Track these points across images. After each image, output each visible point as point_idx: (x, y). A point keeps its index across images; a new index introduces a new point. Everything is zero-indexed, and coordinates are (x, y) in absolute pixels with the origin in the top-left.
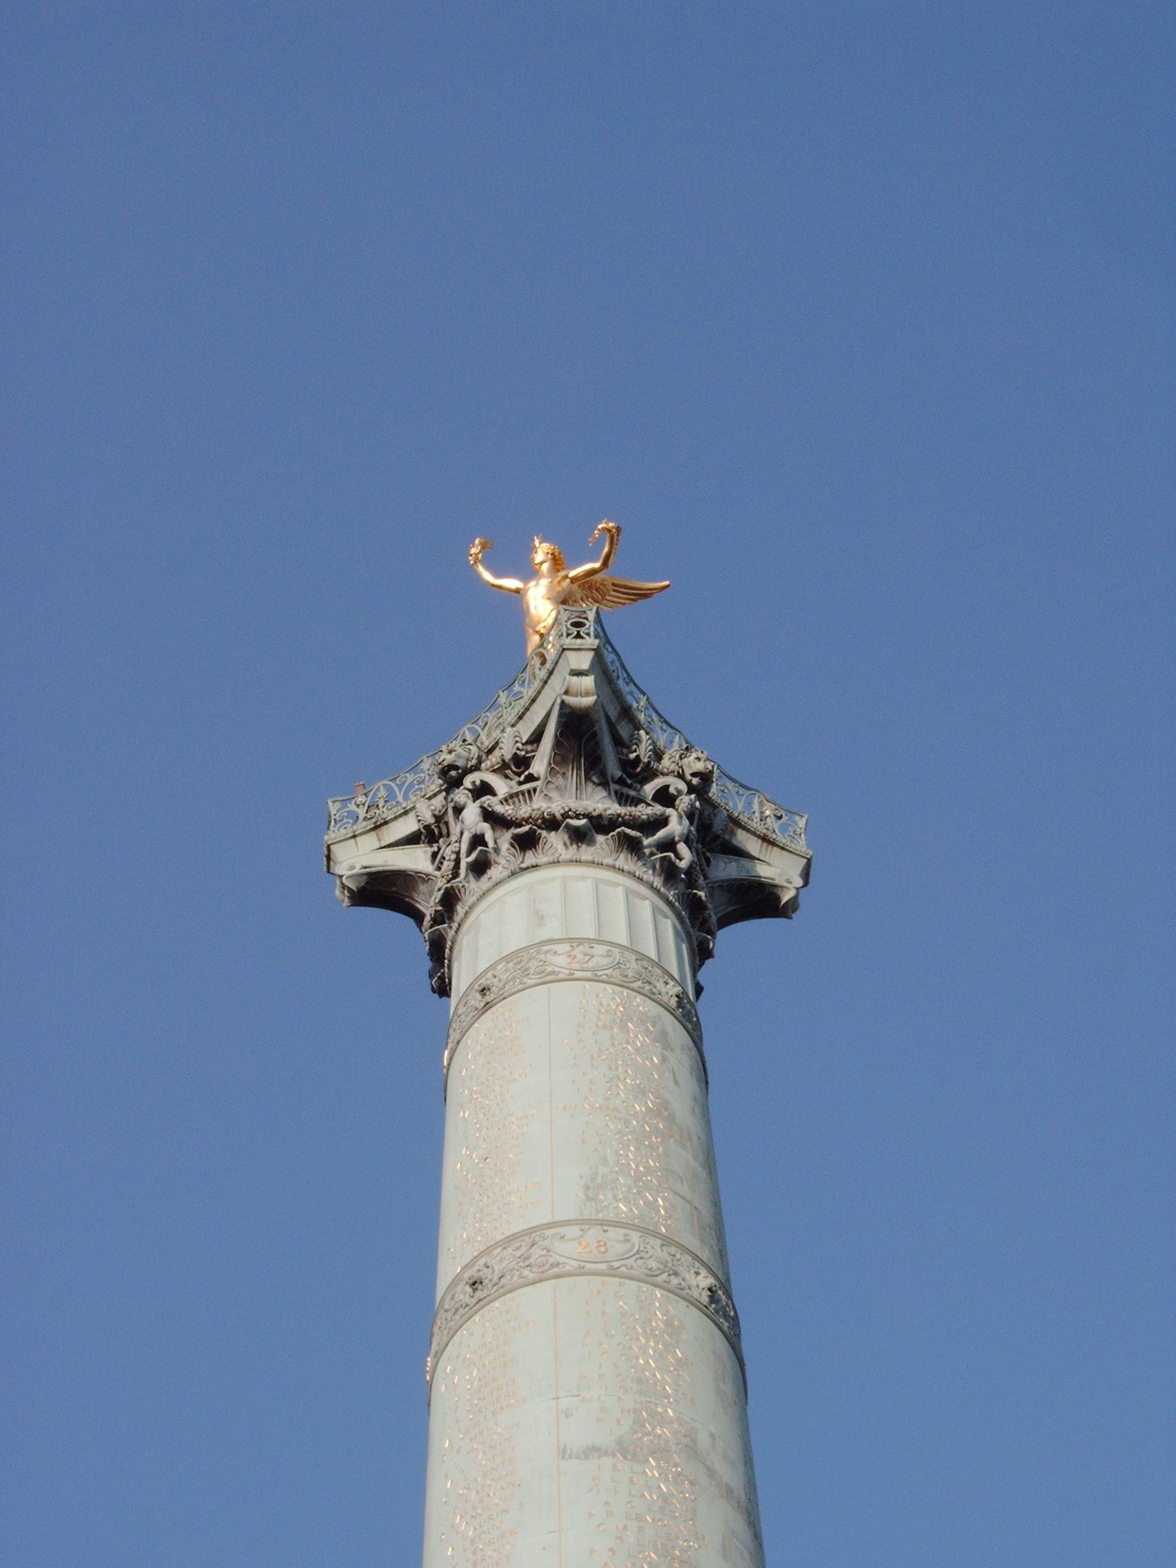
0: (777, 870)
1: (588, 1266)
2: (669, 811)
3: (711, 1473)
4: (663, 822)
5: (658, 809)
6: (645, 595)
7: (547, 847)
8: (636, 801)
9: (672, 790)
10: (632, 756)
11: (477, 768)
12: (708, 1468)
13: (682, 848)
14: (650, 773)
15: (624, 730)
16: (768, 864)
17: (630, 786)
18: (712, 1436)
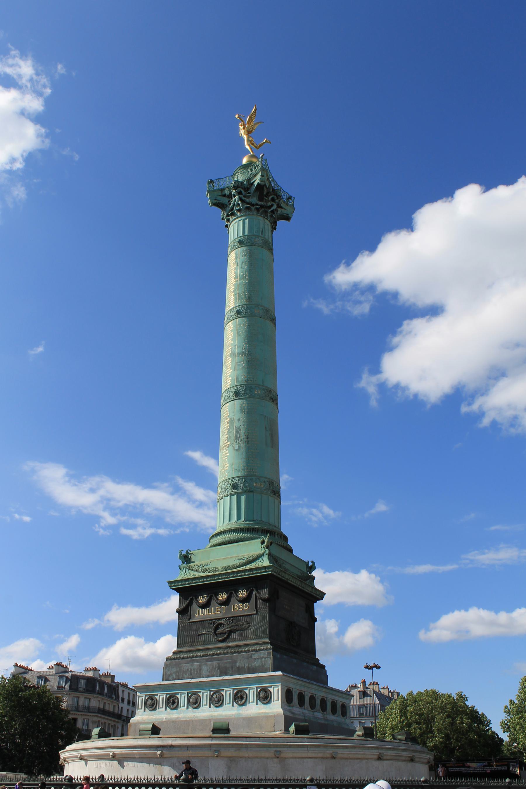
4: (272, 205)
5: (272, 203)
11: (239, 187)
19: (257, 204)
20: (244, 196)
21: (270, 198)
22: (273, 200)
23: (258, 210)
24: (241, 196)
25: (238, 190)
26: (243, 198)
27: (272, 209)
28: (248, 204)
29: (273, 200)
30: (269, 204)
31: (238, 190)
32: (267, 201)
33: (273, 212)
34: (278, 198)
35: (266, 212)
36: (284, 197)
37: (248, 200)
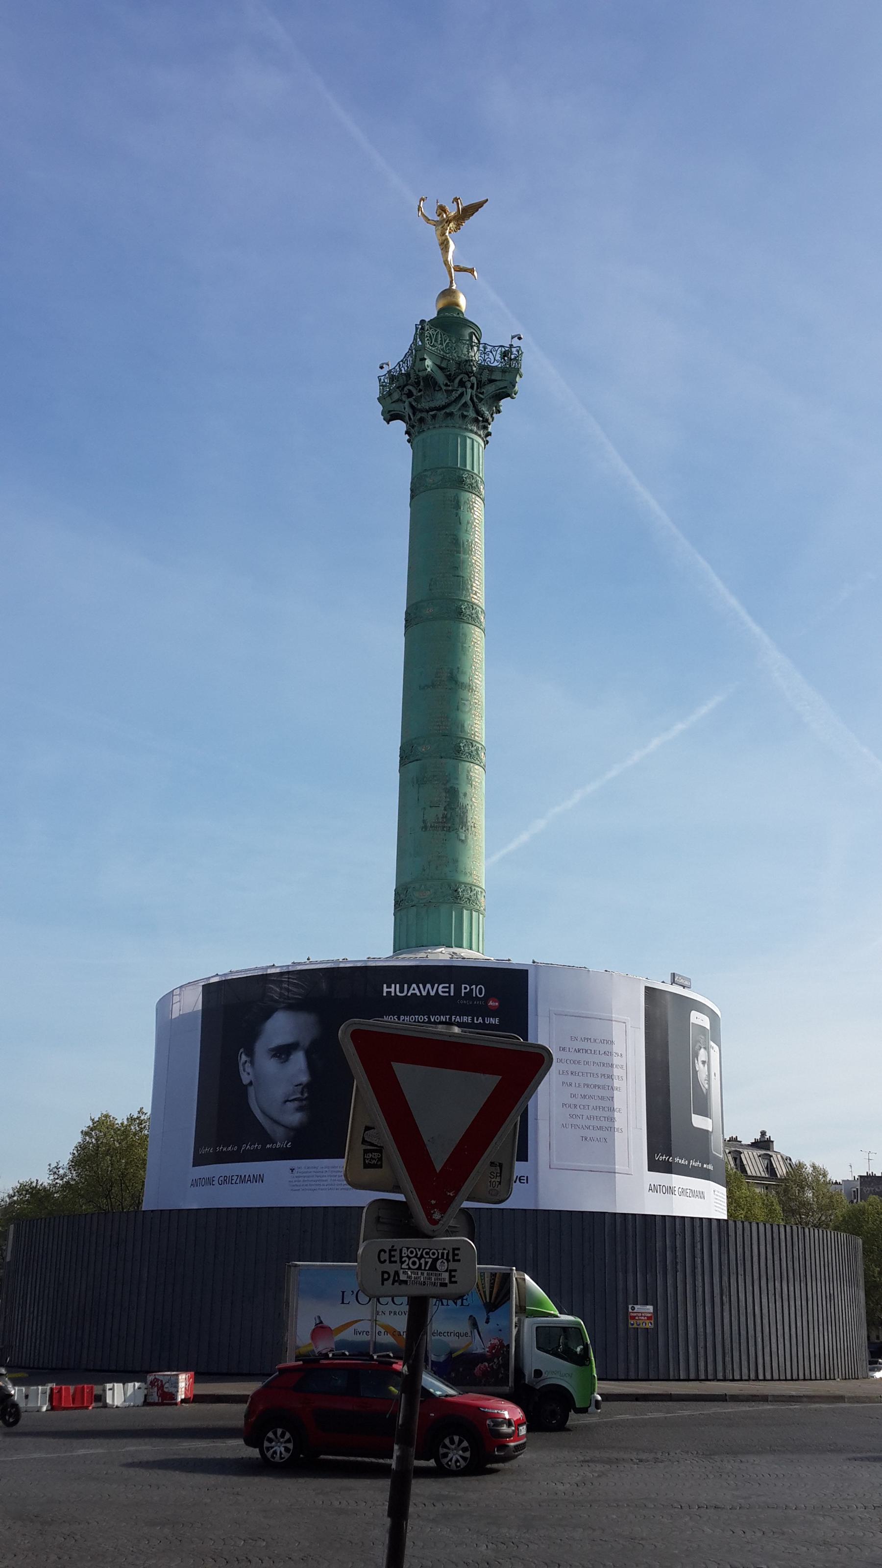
4: (462, 395)
5: (460, 390)
6: (480, 205)
8: (452, 391)
15: (444, 365)
19: (432, 409)
20: (415, 400)
21: (457, 381)
24: (411, 399)
25: (405, 389)
26: (414, 404)
27: (463, 401)
28: (421, 411)
29: (462, 384)
30: (455, 395)
32: (449, 392)
33: (465, 405)
35: (451, 414)
36: (494, 360)
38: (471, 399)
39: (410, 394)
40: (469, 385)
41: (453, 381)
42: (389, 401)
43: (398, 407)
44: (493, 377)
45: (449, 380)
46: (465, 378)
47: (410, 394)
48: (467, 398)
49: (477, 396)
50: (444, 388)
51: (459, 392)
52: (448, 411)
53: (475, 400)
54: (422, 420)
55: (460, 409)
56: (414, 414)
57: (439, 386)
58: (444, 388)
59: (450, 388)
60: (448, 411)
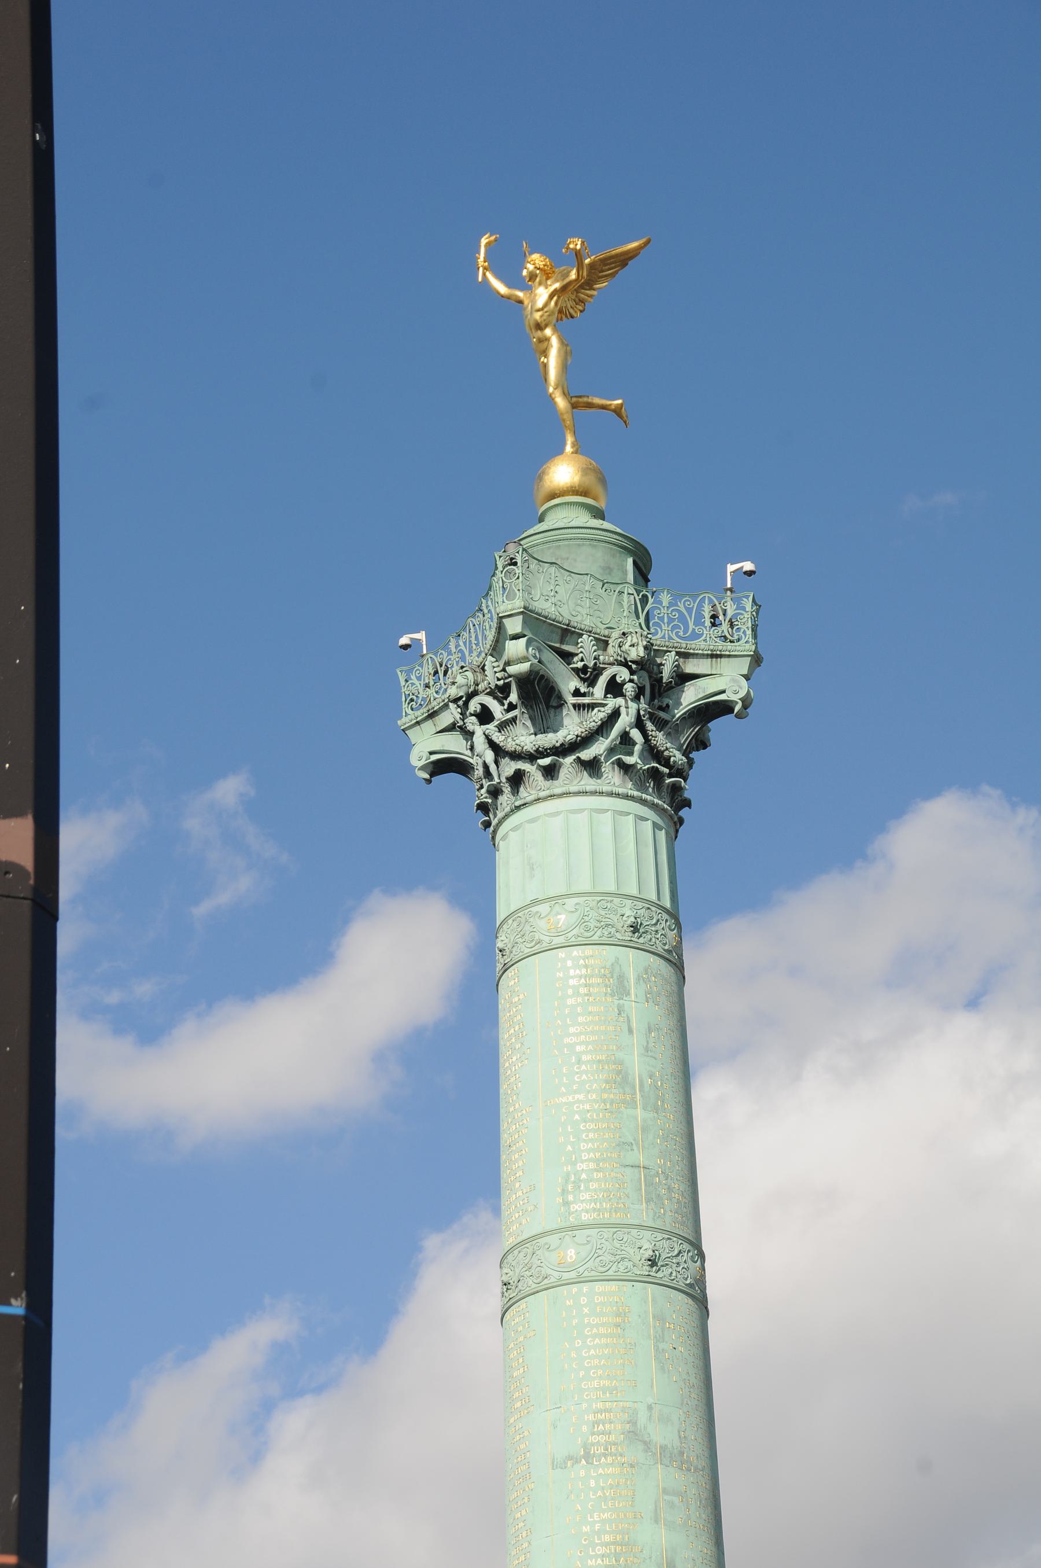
0: (726, 680)
1: (566, 1276)
2: (620, 701)
3: (647, 1445)
4: (615, 714)
5: (612, 703)
7: (531, 779)
8: (591, 706)
9: (619, 680)
10: (580, 665)
11: (475, 693)
12: (645, 1443)
13: (636, 734)
14: (597, 671)
16: (721, 675)
17: (584, 695)
18: (650, 1408)
19: (541, 753)
22: (614, 688)
23: (550, 772)
24: (491, 728)
25: (474, 706)
26: (498, 738)
28: (515, 756)
29: (614, 688)
30: (598, 716)
31: (474, 706)
33: (625, 739)
34: (632, 673)
37: (510, 745)
38: (639, 724)
39: (485, 716)
40: (629, 689)
41: (592, 682)
42: (429, 727)
43: (454, 745)
44: (690, 667)
45: (584, 680)
46: (623, 674)
47: (485, 716)
48: (625, 720)
49: (652, 717)
50: (571, 700)
51: (608, 709)
52: (586, 754)
53: (649, 726)
54: (517, 780)
55: (611, 751)
56: (496, 762)
57: (560, 697)
58: (571, 700)
59: (586, 700)
60: (586, 754)
